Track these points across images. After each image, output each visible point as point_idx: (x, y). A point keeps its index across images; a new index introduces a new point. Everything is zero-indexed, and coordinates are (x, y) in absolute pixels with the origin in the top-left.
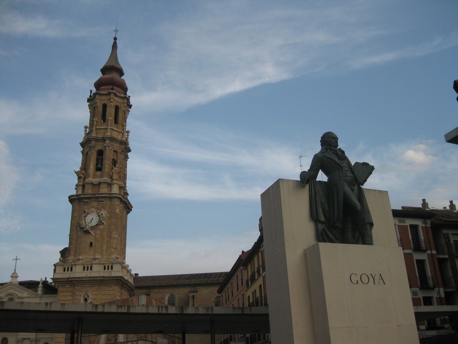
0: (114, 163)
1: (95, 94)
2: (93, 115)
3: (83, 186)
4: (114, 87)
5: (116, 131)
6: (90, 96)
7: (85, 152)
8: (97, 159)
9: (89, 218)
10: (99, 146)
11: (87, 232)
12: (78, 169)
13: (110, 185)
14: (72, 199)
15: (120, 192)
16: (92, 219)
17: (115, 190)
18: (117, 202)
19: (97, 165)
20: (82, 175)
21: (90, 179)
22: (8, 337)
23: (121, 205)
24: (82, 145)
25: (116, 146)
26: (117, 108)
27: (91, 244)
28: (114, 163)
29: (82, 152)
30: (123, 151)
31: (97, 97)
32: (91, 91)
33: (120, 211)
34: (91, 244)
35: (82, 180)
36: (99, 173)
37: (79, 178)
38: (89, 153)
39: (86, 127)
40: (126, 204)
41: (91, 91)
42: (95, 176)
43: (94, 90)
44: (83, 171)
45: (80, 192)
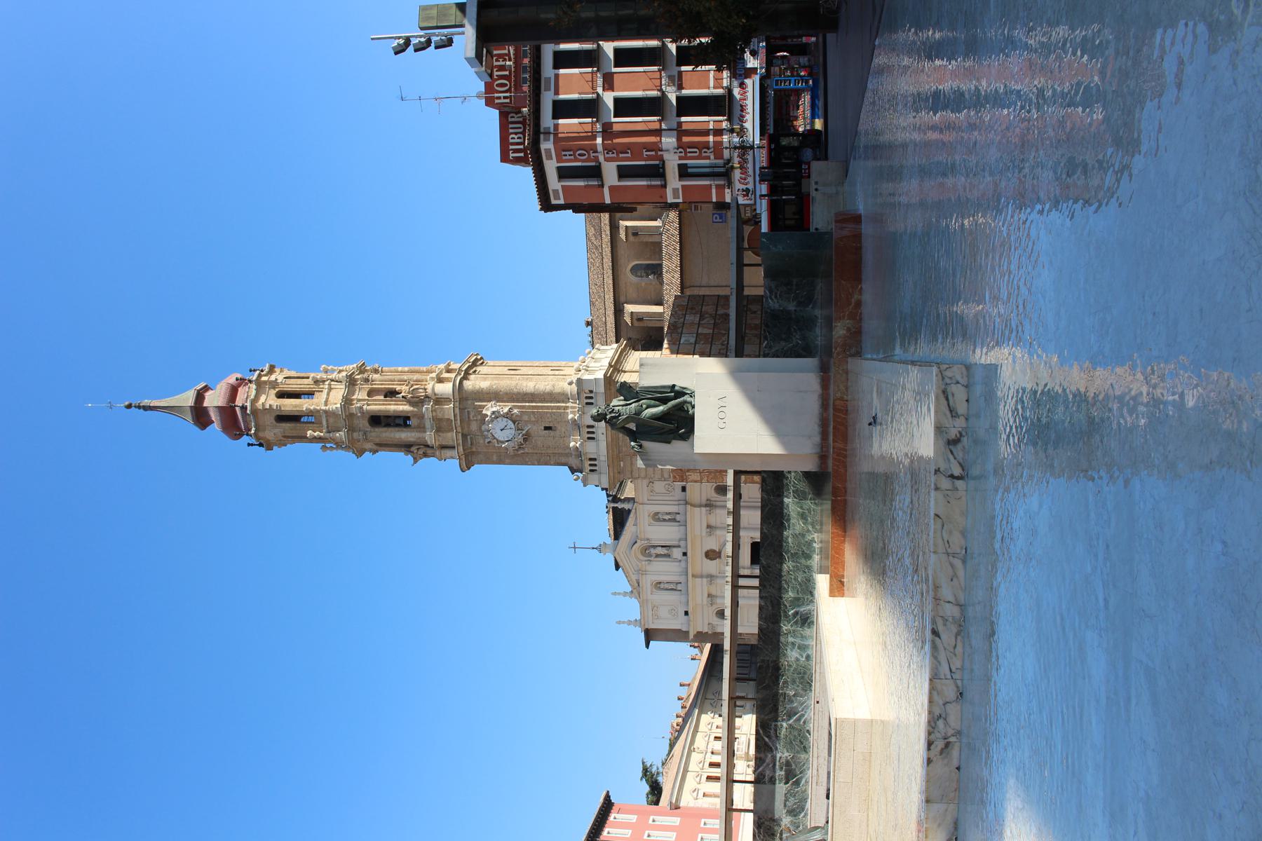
0: (391, 394)
1: (258, 438)
2: (302, 438)
3: (443, 447)
4: (239, 402)
5: (328, 394)
6: (261, 445)
7: (375, 447)
8: (388, 425)
9: (501, 436)
10: (364, 424)
11: (527, 437)
12: (410, 458)
13: (439, 400)
14: (467, 464)
15: (448, 380)
16: (503, 433)
17: (446, 389)
18: (468, 385)
19: (398, 425)
20: (421, 452)
21: (430, 437)
22: (705, 550)
23: (472, 377)
24: (360, 453)
25: (360, 394)
26: (281, 395)
27: (547, 428)
28: (391, 394)
29: (375, 452)
30: (367, 380)
31: (261, 434)
32: (249, 445)
33: (485, 379)
34: (547, 428)
35: (429, 451)
36: (412, 422)
37: (425, 455)
38: (377, 441)
39: (324, 448)
40: (470, 368)
41: (249, 445)
42: (421, 428)
43: (245, 439)
44: (413, 449)
45: (454, 453)
